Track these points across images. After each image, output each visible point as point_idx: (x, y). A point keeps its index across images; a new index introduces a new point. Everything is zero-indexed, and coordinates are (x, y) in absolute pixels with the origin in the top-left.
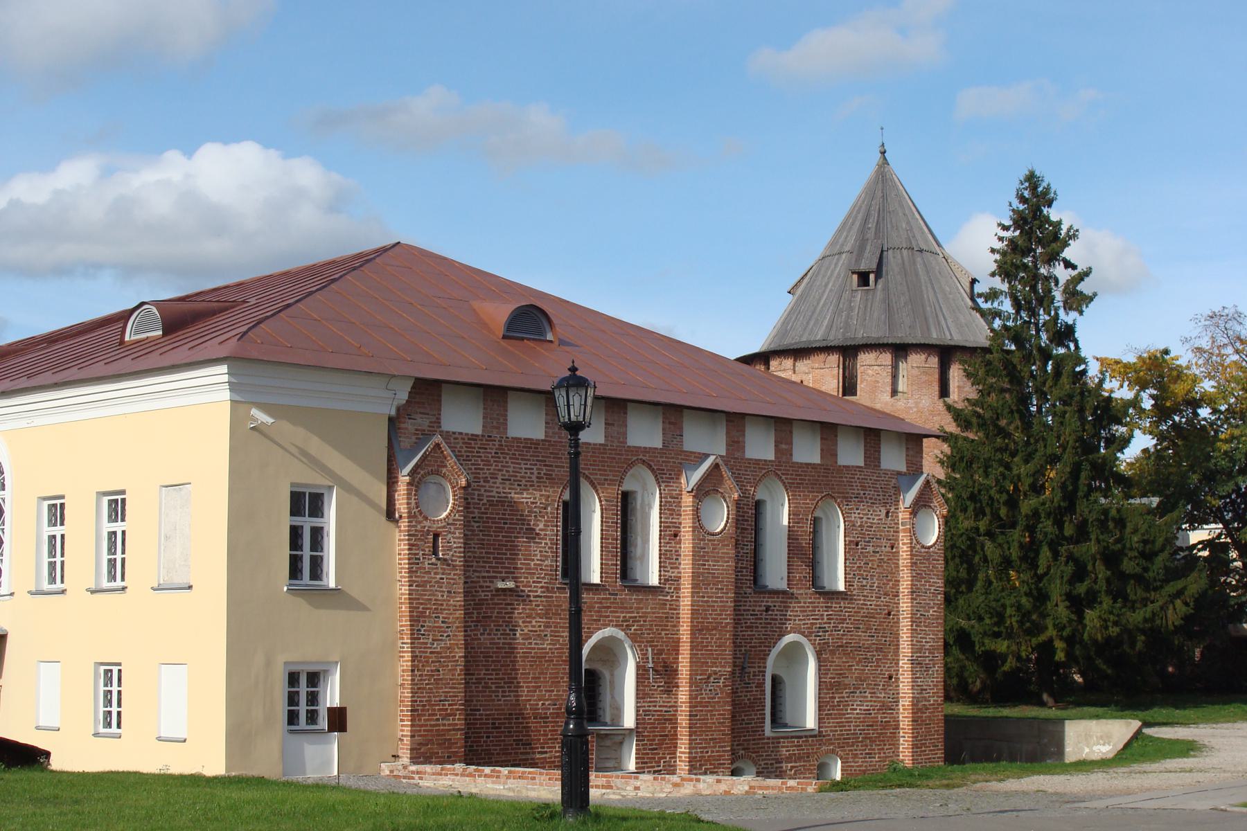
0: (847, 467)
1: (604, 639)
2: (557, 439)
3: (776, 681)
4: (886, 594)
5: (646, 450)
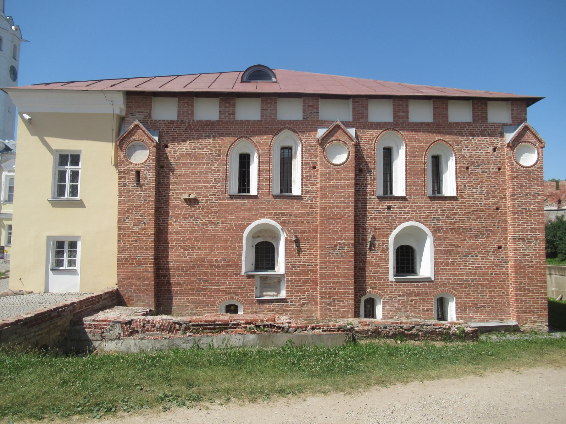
0: (457, 124)
2: (227, 119)
4: (494, 197)
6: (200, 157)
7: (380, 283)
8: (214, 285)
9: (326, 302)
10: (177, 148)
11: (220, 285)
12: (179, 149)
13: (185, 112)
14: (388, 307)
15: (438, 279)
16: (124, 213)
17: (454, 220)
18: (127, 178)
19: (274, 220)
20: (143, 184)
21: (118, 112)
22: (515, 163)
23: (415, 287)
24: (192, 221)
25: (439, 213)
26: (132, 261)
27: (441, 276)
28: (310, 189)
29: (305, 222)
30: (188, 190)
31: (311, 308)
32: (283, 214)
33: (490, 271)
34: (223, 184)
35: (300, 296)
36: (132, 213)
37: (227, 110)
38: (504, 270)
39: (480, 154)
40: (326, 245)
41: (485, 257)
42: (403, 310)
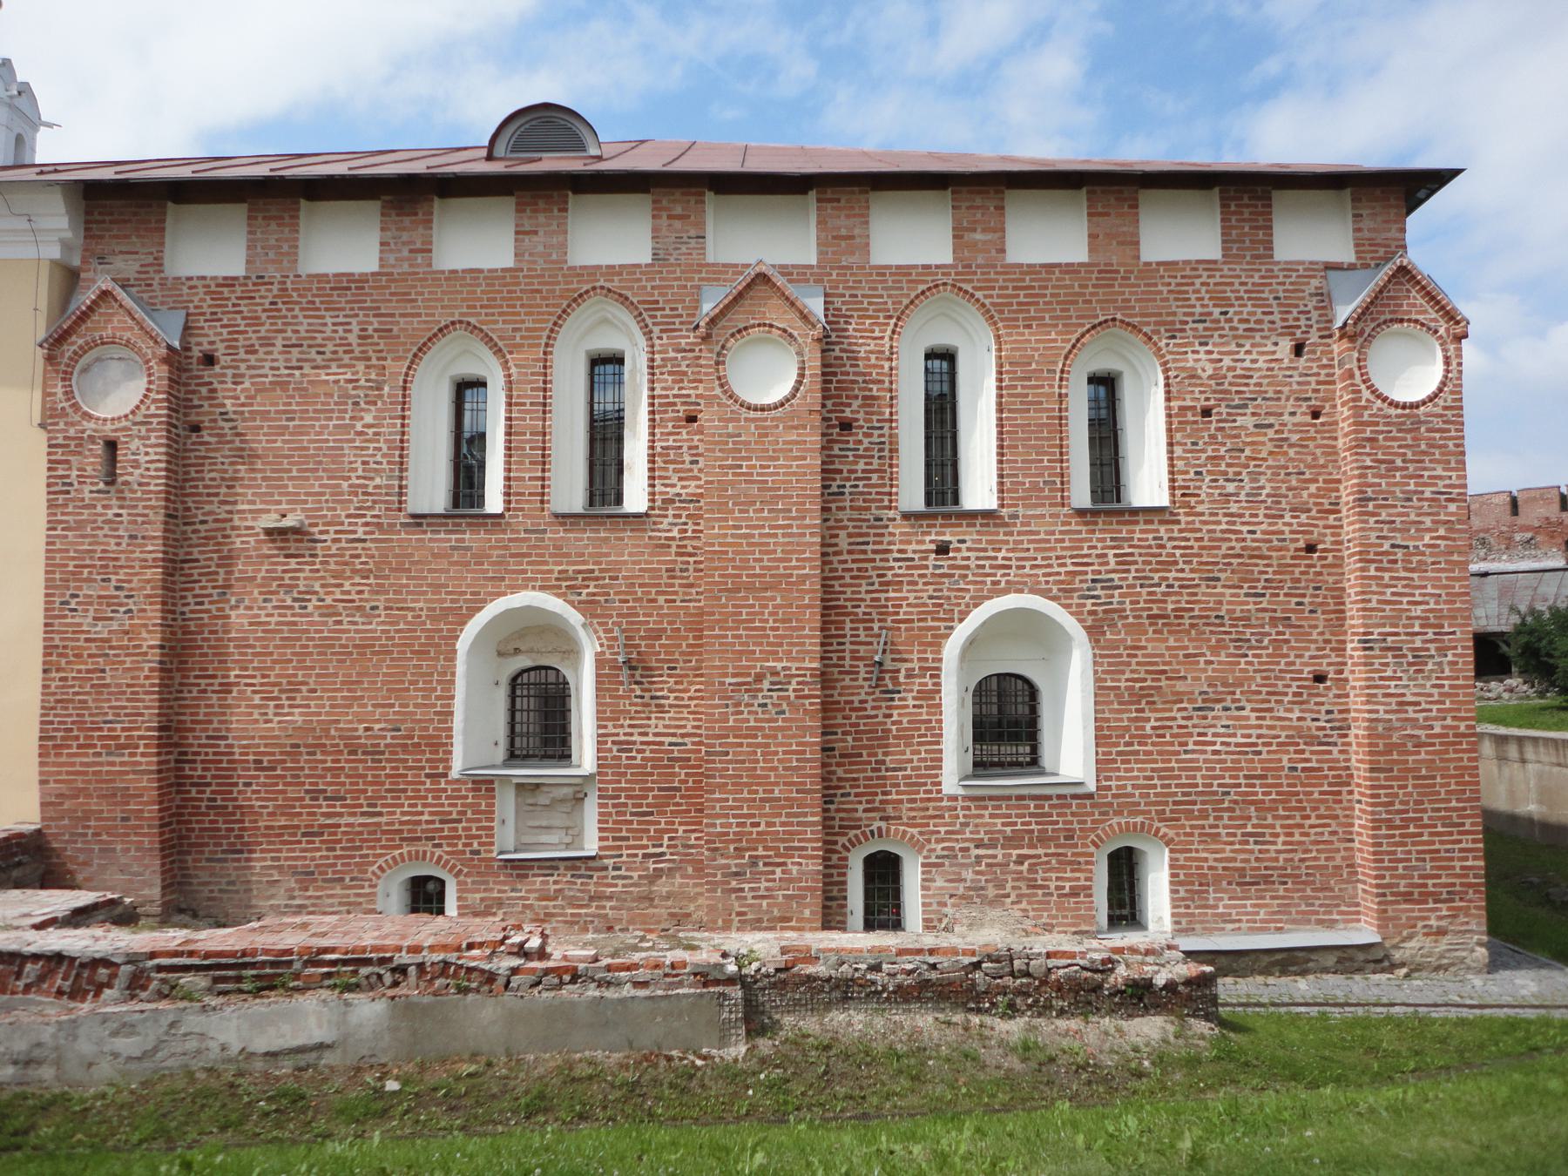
0: (1170, 265)
2: (406, 268)
6: (317, 396)
7: (914, 801)
8: (363, 814)
9: (728, 866)
10: (243, 366)
11: (380, 814)
12: (249, 368)
13: (272, 247)
14: (940, 883)
15: (1109, 788)
16: (63, 581)
17: (1163, 588)
18: (75, 465)
19: (558, 595)
20: (126, 483)
21: (55, 252)
22: (1366, 394)
23: (1031, 815)
24: (289, 602)
25: (1112, 565)
26: (86, 737)
27: (1119, 778)
28: (677, 490)
29: (661, 599)
30: (279, 503)
31: (681, 885)
32: (589, 576)
33: (1285, 758)
34: (390, 478)
35: (646, 847)
36: (88, 580)
37: (405, 236)
38: (1336, 755)
39: (1247, 364)
40: (726, 675)
41: (1270, 710)
42: (991, 892)
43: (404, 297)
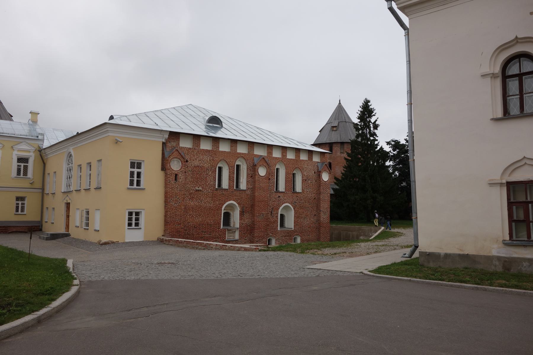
1: (232, 204)
3: (282, 216)
5: (243, 154)
43: (215, 154)
